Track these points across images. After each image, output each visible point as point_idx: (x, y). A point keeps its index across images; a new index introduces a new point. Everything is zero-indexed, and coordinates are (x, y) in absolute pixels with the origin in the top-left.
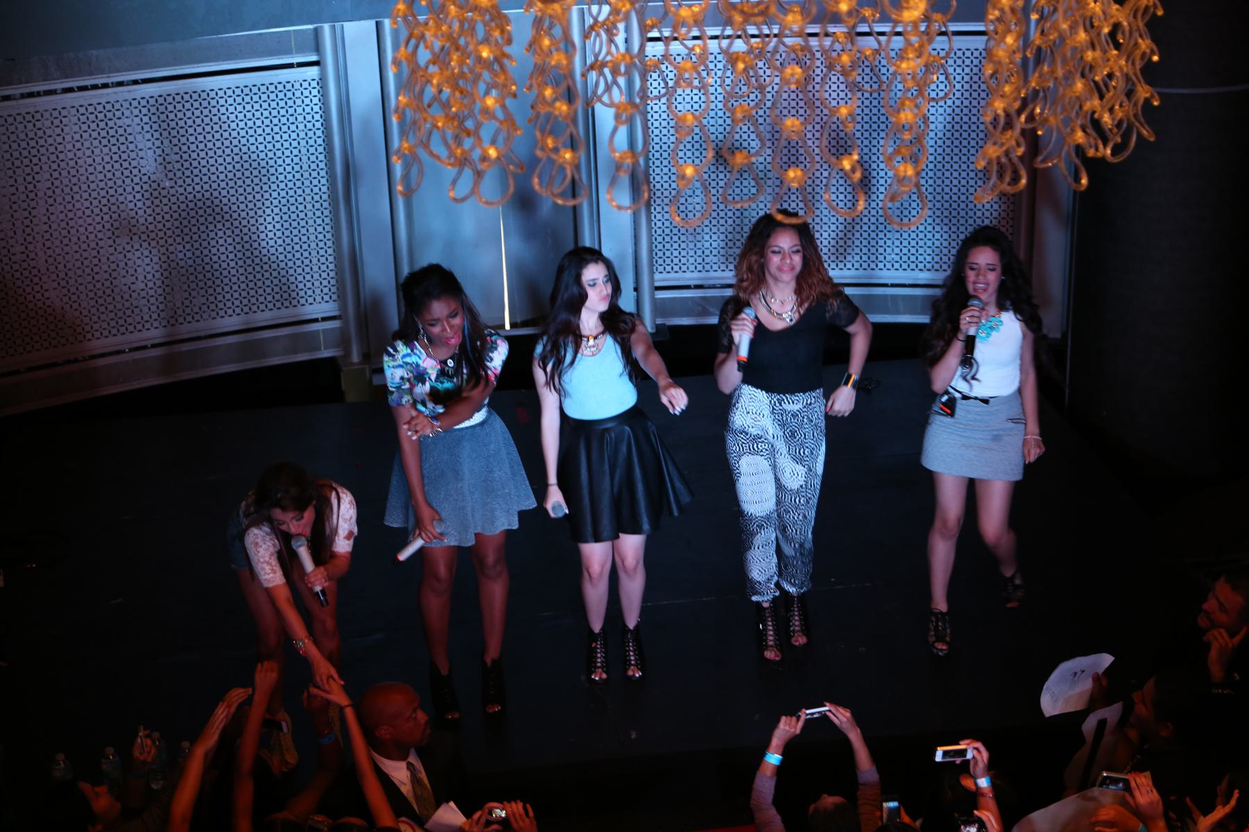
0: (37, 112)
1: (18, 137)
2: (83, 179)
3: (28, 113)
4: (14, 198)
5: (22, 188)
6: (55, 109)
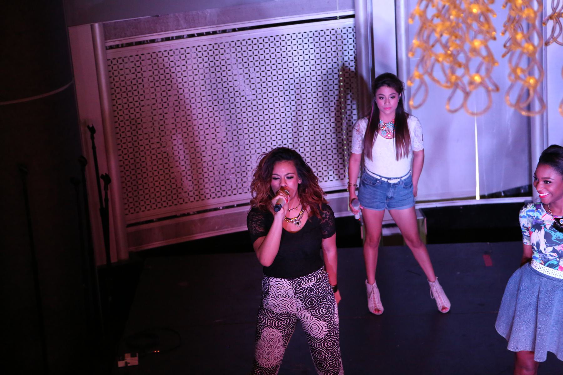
0: (171, 50)
1: (158, 66)
2: (198, 94)
3: (165, 51)
4: (154, 107)
5: (159, 100)
6: (182, 48)
